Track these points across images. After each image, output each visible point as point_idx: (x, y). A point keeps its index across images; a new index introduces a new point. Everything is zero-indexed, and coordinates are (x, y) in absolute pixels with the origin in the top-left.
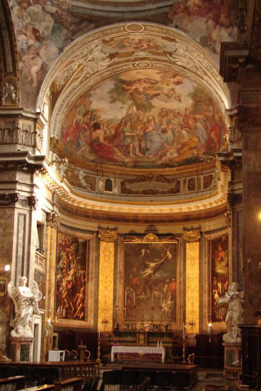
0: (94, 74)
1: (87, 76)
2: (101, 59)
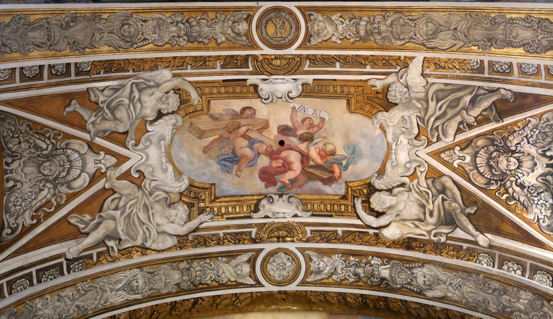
0: (127, 253)
1: (111, 243)
2: (164, 195)
